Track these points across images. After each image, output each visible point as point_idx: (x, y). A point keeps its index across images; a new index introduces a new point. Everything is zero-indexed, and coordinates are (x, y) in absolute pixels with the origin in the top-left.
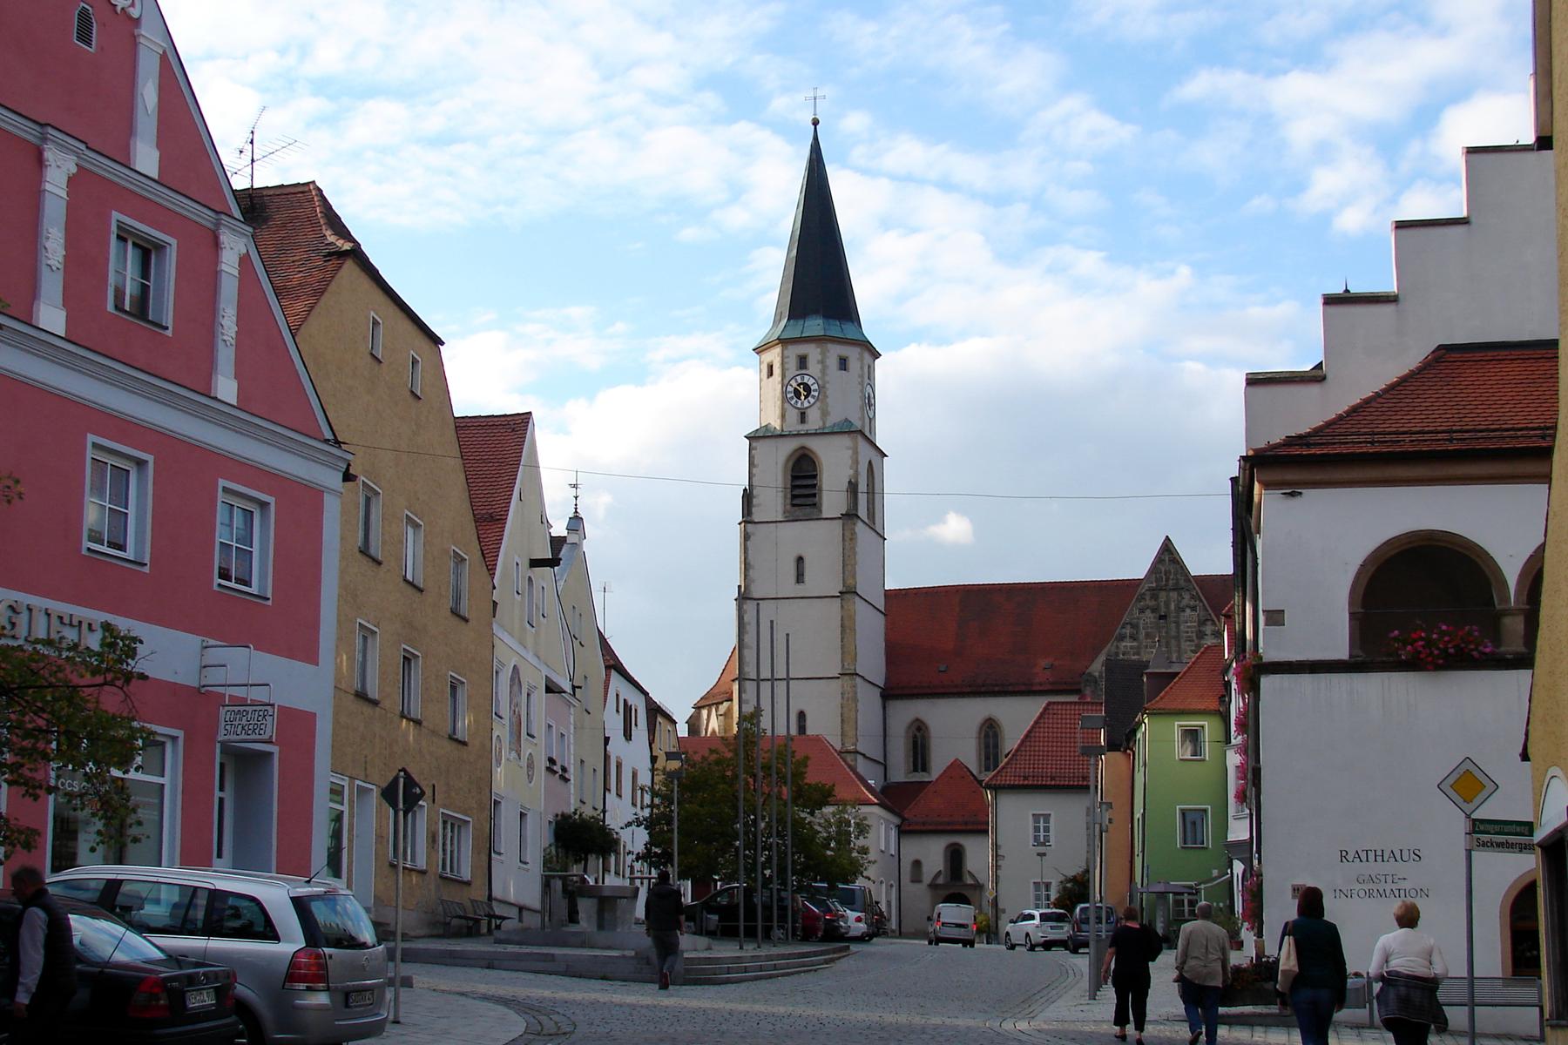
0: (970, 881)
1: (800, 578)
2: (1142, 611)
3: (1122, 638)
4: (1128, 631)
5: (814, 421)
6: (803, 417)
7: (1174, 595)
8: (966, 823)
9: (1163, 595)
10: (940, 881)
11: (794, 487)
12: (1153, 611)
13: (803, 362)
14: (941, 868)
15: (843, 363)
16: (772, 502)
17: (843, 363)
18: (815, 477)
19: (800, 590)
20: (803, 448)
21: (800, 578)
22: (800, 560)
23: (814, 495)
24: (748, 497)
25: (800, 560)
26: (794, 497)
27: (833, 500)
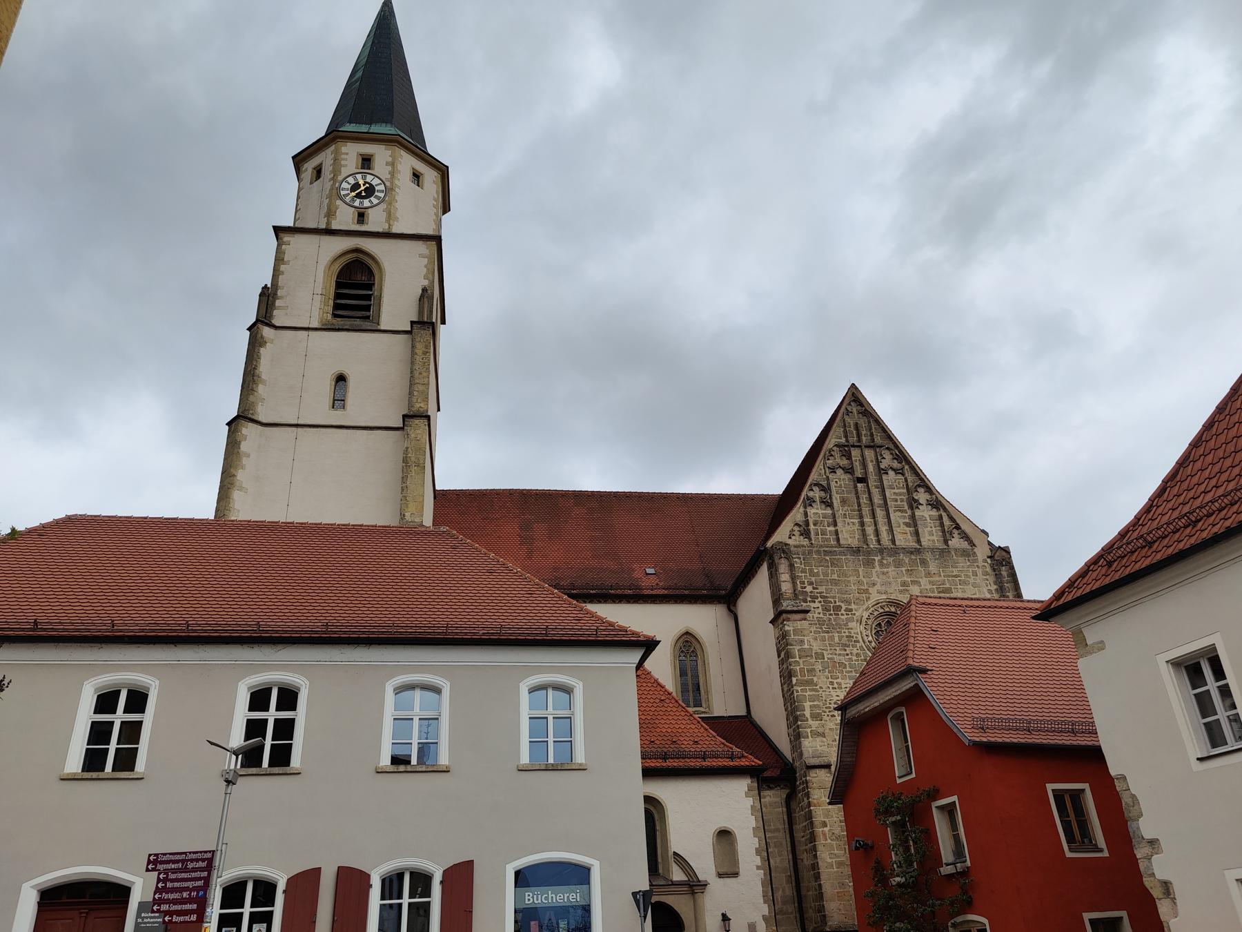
0: (678, 875)
1: (338, 401)
2: (833, 470)
3: (810, 502)
4: (817, 494)
5: (376, 221)
6: (361, 217)
7: (869, 454)
8: (665, 757)
9: (855, 453)
11: (338, 296)
12: (849, 470)
13: (366, 161)
16: (308, 297)
17: (417, 176)
18: (370, 286)
19: (336, 417)
20: (357, 250)
21: (338, 401)
22: (341, 379)
23: (368, 308)
24: (268, 297)
25: (341, 379)
26: (336, 307)
27: (396, 303)
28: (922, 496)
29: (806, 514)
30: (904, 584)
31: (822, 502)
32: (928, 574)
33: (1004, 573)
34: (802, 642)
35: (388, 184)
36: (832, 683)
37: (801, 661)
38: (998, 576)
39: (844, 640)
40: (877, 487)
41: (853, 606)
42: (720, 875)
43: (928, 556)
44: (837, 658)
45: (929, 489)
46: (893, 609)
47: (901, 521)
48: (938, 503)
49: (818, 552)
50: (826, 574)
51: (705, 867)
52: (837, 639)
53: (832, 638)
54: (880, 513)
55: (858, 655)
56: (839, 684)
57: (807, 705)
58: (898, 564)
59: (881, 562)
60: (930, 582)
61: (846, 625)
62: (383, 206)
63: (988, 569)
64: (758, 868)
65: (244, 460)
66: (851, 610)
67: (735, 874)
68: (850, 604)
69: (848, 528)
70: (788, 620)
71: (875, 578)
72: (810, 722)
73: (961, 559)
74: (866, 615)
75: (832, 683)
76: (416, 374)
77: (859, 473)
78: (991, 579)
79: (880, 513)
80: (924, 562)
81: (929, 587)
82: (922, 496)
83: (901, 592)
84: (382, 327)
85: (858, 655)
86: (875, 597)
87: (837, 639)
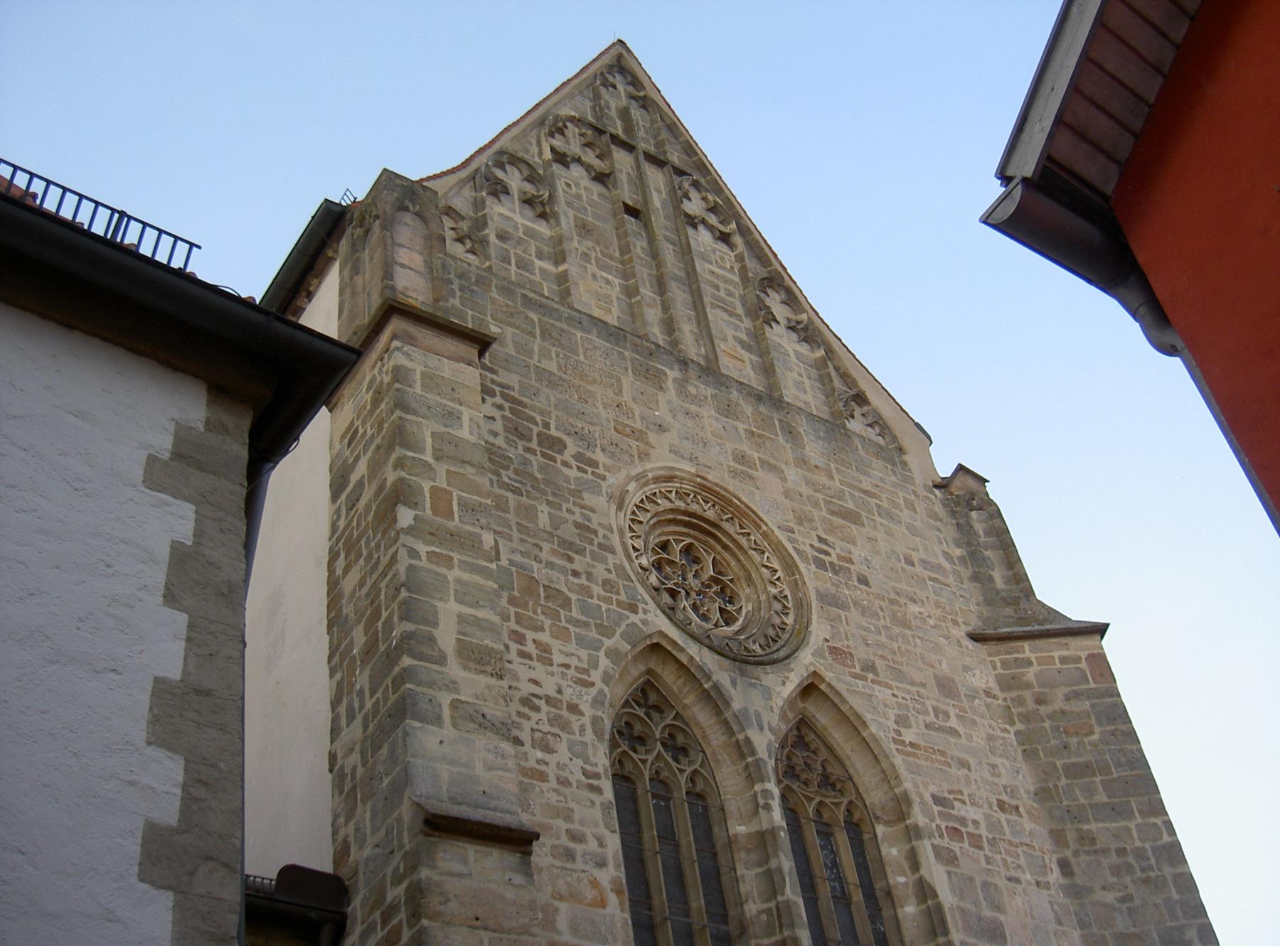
2: (561, 158)
28: (774, 301)
29: (479, 205)
30: (741, 458)
31: (528, 201)
32: (802, 462)
33: (979, 528)
34: (452, 417)
36: (520, 639)
37: (442, 469)
38: (965, 529)
39: (568, 531)
40: (668, 239)
41: (599, 456)
43: (802, 426)
44: (539, 571)
45: (793, 298)
46: (711, 514)
47: (730, 332)
48: (810, 331)
49: (507, 290)
50: (525, 350)
52: (544, 520)
53: (531, 513)
54: (679, 295)
55: (606, 584)
56: (544, 649)
57: (449, 610)
58: (728, 410)
59: (682, 384)
60: (808, 482)
61: (577, 493)
63: (939, 509)
66: (593, 464)
68: (591, 446)
69: (594, 286)
70: (411, 341)
71: (662, 413)
72: (454, 669)
73: (878, 464)
74: (635, 495)
75: (520, 639)
77: (627, 194)
78: (950, 531)
79: (679, 295)
80: (790, 432)
81: (805, 490)
82: (774, 301)
83: (735, 474)
85: (606, 584)
86: (661, 460)
87: (544, 520)
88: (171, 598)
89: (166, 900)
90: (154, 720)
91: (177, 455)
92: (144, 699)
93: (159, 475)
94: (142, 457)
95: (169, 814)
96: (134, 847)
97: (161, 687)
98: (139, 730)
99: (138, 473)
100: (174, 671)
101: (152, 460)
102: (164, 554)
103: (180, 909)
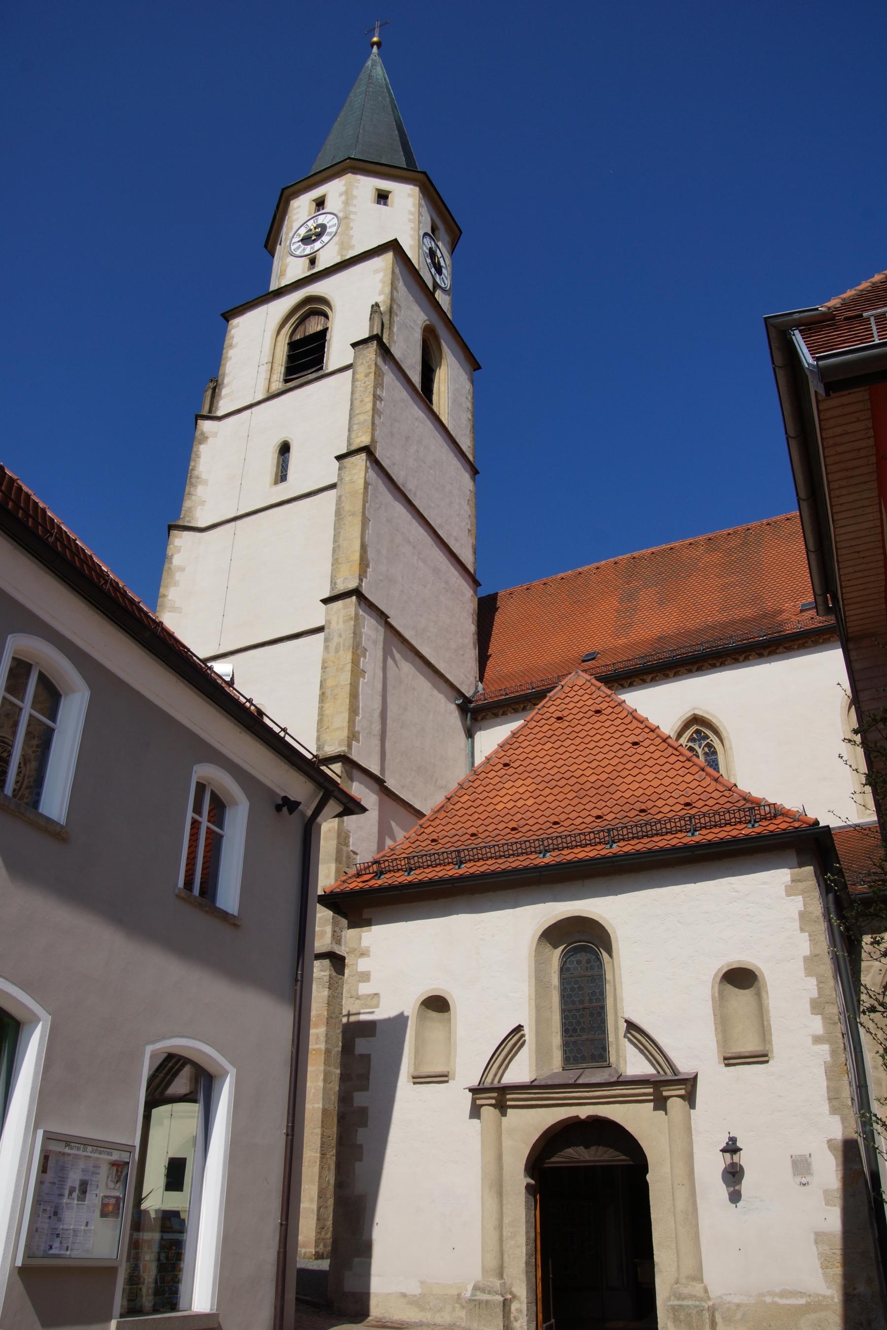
0: (634, 1064)
1: (282, 476)
10: (520, 1071)
13: (320, 203)
14: (524, 1016)
15: (382, 197)
17: (382, 197)
21: (282, 476)
22: (285, 449)
25: (285, 449)
35: (341, 215)
42: (730, 1060)
51: (691, 1045)
62: (336, 239)
64: (817, 1040)
65: (178, 576)
67: (761, 1058)
76: (357, 403)
84: (331, 368)
88: (802, 930)
89: (819, 1017)
90: (806, 969)
91: (793, 881)
92: (801, 964)
93: (790, 891)
94: (783, 887)
95: (815, 994)
96: (808, 1006)
97: (806, 959)
98: (802, 973)
99: (784, 893)
100: (807, 953)
101: (786, 886)
102: (797, 916)
103: (824, 1019)
